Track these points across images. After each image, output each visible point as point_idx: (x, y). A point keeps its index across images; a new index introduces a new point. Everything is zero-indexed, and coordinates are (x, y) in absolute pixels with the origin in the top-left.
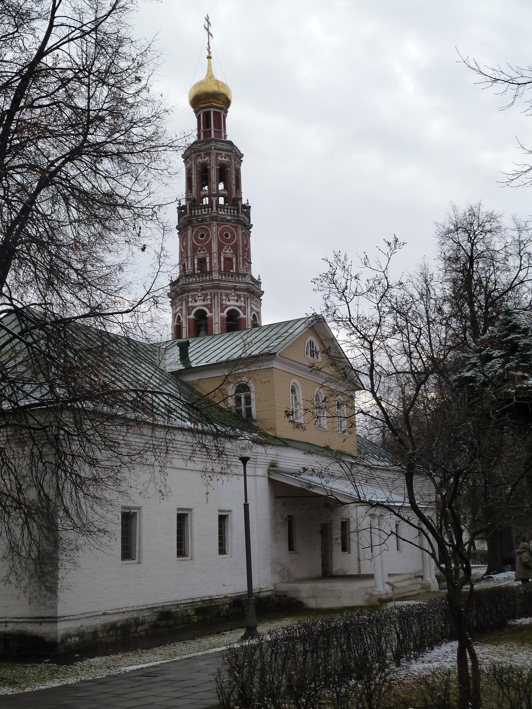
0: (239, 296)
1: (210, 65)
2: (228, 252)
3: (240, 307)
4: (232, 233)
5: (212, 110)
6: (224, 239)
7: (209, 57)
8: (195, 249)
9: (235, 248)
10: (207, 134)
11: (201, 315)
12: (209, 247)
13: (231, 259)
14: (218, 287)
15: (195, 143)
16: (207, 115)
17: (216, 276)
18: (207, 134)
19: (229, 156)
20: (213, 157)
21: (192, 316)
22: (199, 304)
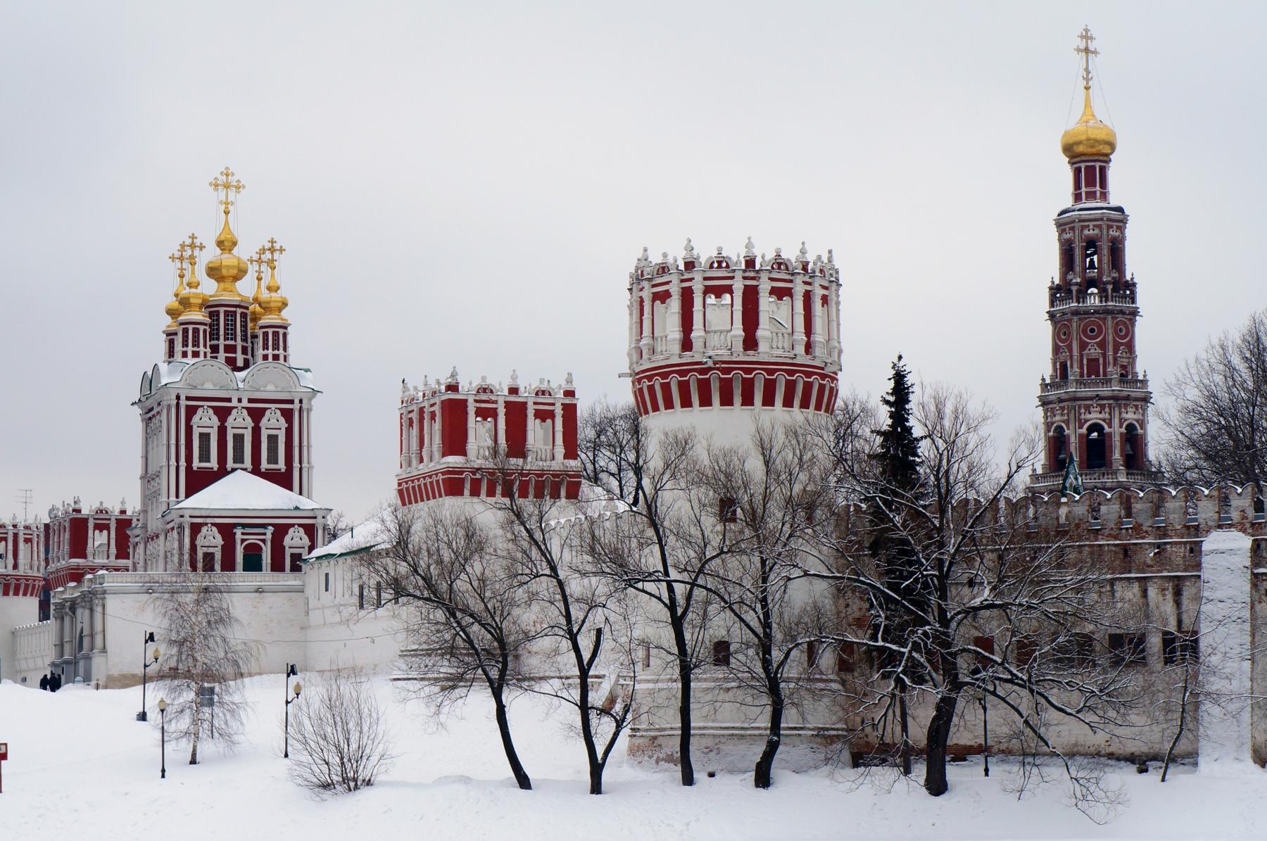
0: (1103, 407)
1: (1088, 99)
3: (1104, 420)
5: (1083, 165)
7: (1087, 88)
9: (1102, 345)
12: (1070, 348)
13: (1097, 360)
19: (1100, 227)
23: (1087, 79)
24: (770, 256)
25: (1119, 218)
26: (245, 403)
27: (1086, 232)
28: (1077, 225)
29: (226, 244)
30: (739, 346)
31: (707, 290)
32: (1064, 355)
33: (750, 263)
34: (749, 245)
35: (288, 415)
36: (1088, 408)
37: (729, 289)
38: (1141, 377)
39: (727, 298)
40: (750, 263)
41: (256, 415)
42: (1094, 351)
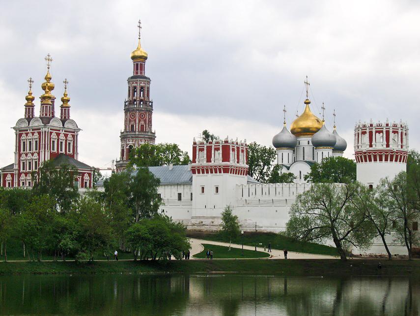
0: (146, 141)
2: (142, 123)
4: (144, 115)
5: (139, 63)
6: (140, 115)
8: (130, 121)
9: (145, 121)
10: (137, 73)
11: (131, 147)
12: (135, 120)
14: (138, 137)
15: (132, 78)
16: (137, 65)
17: (137, 133)
18: (137, 73)
20: (138, 84)
21: (128, 147)
22: (131, 143)
23: (140, 36)
24: (393, 123)
25: (148, 81)
26: (63, 132)
27: (141, 84)
28: (138, 82)
29: (48, 79)
30: (385, 146)
31: (376, 132)
32: (132, 123)
33: (387, 125)
34: (387, 120)
35: (73, 136)
36: (141, 140)
37: (382, 132)
38: (153, 132)
39: (381, 134)
40: (387, 125)
41: (66, 136)
42: (142, 123)
